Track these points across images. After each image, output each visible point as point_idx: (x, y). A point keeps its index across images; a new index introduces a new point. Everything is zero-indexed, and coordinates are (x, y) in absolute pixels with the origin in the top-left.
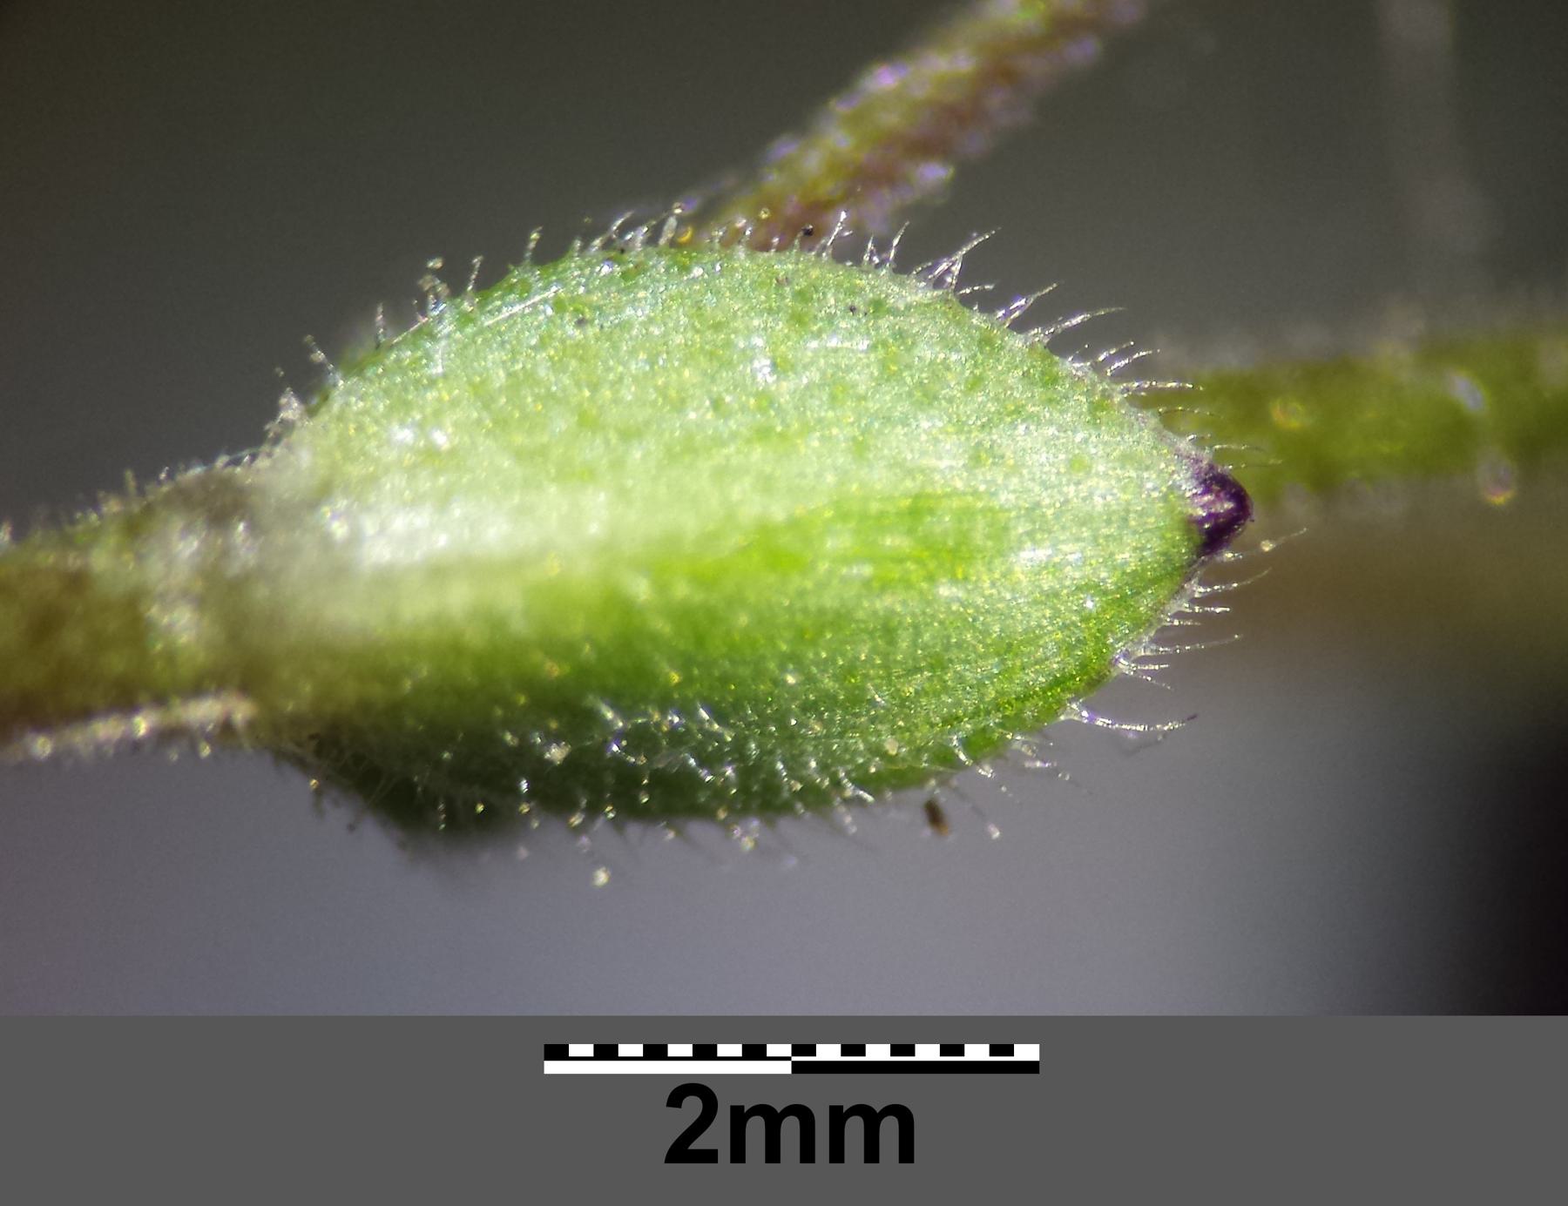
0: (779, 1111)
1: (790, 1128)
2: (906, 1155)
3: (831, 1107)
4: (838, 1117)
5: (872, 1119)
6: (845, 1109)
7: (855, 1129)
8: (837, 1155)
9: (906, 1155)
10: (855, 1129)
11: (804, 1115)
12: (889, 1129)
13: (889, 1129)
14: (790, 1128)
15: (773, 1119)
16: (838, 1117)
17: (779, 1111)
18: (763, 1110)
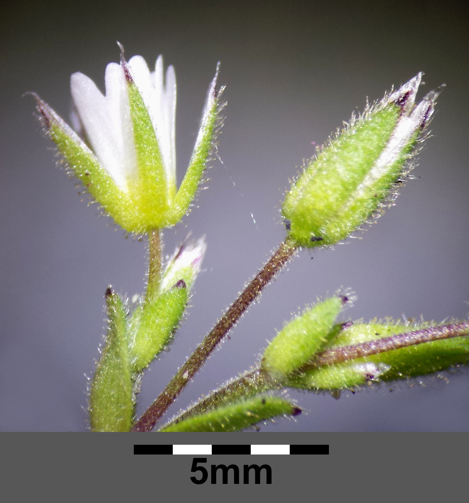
0: (260, 467)
1: (231, 472)
2: (269, 481)
3: (212, 465)
4: (247, 469)
5: (225, 469)
6: (249, 466)
7: (252, 472)
8: (246, 481)
9: (269, 481)
10: (252, 472)
11: (236, 468)
12: (263, 472)
13: (263, 472)
14: (231, 472)
15: (258, 469)
16: (247, 469)
17: (260, 467)
18: (254, 466)
